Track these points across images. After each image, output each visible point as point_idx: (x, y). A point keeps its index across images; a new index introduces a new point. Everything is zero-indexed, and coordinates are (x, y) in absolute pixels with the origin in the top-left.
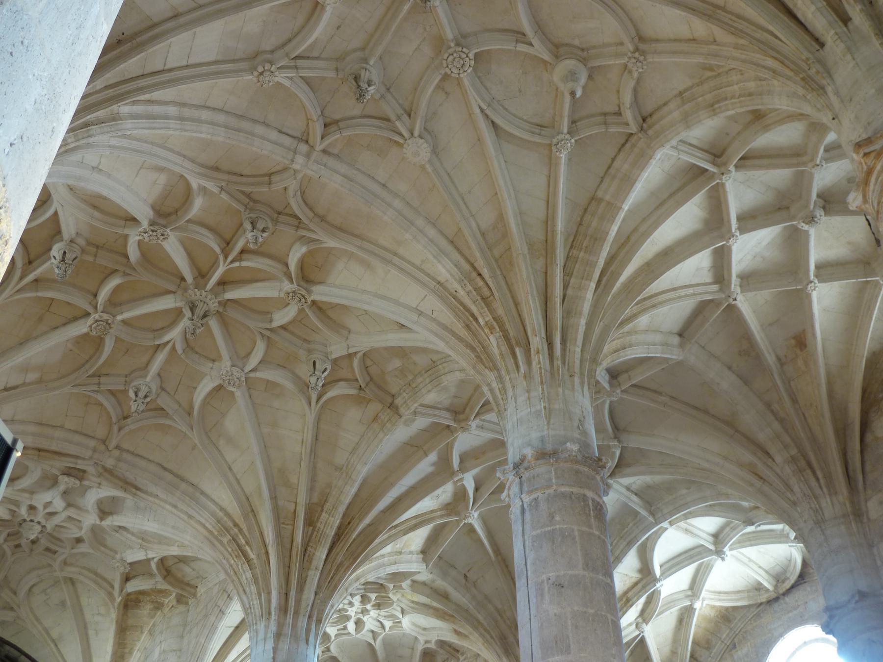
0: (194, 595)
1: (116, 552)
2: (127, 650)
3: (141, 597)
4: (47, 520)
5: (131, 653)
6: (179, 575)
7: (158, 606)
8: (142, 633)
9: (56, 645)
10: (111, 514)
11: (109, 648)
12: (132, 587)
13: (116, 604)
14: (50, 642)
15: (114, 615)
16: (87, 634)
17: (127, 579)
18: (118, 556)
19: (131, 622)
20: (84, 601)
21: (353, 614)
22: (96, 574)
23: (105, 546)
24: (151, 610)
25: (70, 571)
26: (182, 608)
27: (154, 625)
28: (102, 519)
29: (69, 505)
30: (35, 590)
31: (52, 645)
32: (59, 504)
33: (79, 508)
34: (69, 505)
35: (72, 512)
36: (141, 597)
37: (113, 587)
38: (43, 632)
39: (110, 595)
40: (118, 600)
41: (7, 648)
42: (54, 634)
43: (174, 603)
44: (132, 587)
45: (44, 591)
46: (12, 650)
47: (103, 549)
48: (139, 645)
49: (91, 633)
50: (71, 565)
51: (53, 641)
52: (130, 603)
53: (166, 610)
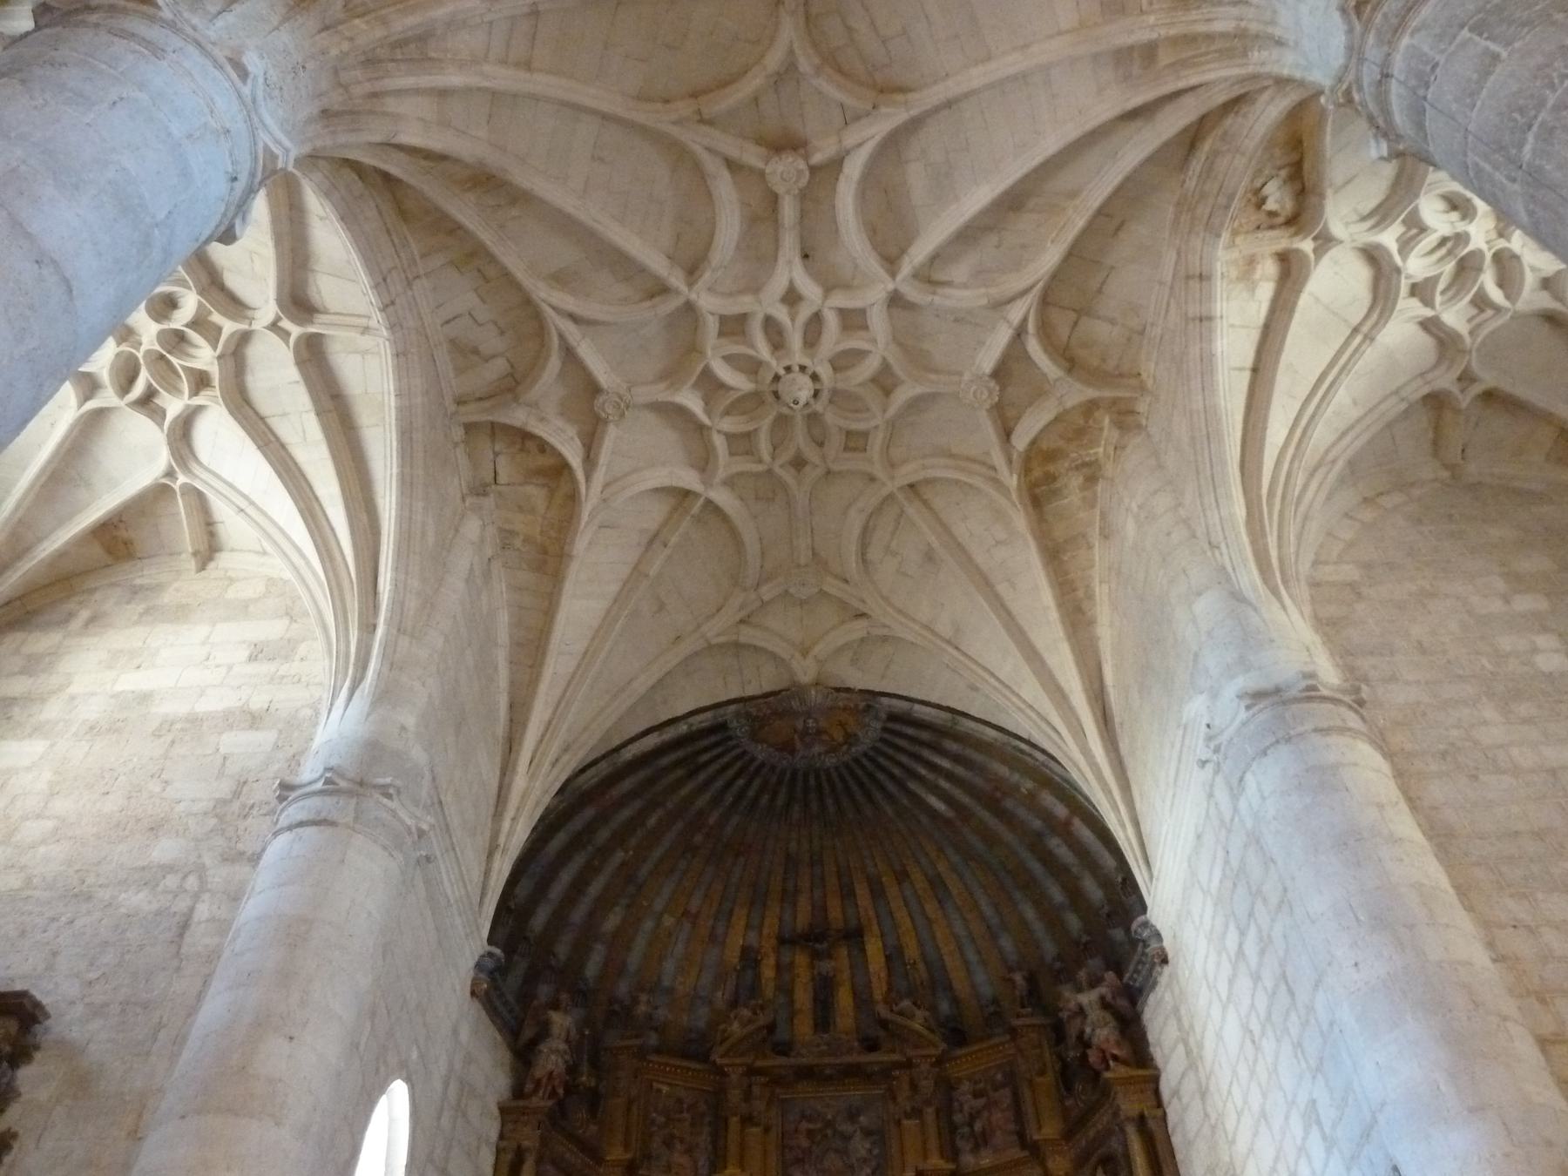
0: (1142, 388)
1: (960, 374)
2: (1080, 593)
3: (1051, 468)
4: (812, 357)
5: (1090, 596)
6: (1095, 362)
7: (1092, 474)
8: (1090, 547)
9: (957, 648)
10: (903, 251)
11: (1047, 597)
12: (1021, 441)
13: (1014, 496)
14: (944, 645)
15: (1020, 521)
16: (997, 597)
17: (1007, 434)
18: (967, 377)
19: (1060, 532)
20: (960, 531)
21: (1484, 247)
22: (952, 456)
23: (936, 371)
24: (1083, 488)
25: (909, 472)
26: (1135, 440)
27: (1103, 515)
28: (893, 275)
29: (828, 290)
30: (874, 553)
31: (950, 649)
32: (810, 290)
33: (847, 287)
34: (828, 290)
35: (840, 300)
36: (1051, 468)
37: (994, 468)
38: (925, 633)
39: (997, 483)
40: (1012, 481)
41: (885, 700)
42: (944, 628)
43: (1116, 434)
44: (1021, 441)
46: (895, 702)
47: (933, 377)
48: (1096, 573)
49: (1002, 588)
50: (904, 462)
51: (949, 642)
52: (1039, 495)
53: (1109, 469)
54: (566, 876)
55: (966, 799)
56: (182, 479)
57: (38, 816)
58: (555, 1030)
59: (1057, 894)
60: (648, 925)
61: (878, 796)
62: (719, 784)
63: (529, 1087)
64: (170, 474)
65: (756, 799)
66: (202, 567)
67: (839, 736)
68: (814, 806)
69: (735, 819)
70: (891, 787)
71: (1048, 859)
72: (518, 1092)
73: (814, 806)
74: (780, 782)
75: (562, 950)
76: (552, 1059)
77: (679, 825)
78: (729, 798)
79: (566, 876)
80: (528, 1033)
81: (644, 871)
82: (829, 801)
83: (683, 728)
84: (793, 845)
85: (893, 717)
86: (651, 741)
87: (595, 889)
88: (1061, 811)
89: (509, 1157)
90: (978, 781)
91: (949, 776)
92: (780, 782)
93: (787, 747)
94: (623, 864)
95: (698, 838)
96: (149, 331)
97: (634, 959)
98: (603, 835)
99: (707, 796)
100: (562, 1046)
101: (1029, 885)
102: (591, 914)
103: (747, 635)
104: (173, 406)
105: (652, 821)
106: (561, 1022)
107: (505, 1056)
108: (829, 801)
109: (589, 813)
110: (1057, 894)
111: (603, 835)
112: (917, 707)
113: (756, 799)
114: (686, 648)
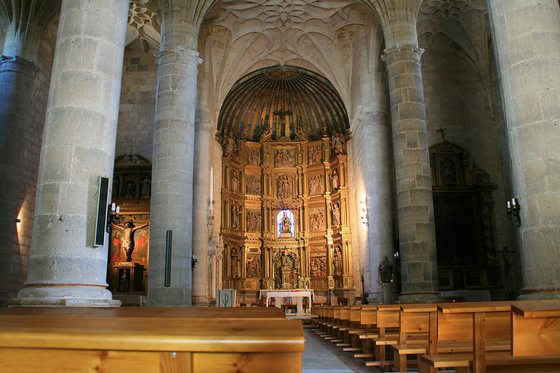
41: (300, 70)
45: (303, 42)
54: (228, 107)
55: (317, 90)
56: (142, 38)
57: (139, 124)
58: (230, 143)
59: (335, 113)
60: (245, 112)
61: (298, 86)
62: (261, 84)
63: (226, 154)
64: (139, 37)
65: (270, 85)
66: (146, 53)
67: (289, 75)
68: (283, 87)
69: (264, 90)
70: (301, 85)
71: (334, 106)
72: (224, 155)
73: (283, 87)
74: (275, 82)
75: (228, 122)
76: (230, 149)
77: (252, 92)
78: (263, 86)
79: (228, 107)
80: (225, 142)
81: (244, 102)
82: (286, 86)
83: (254, 75)
84: (277, 94)
85: (302, 73)
86: (247, 78)
87: (234, 108)
88: (337, 99)
89: (224, 168)
90: (321, 88)
91: (314, 85)
92: (275, 82)
93: (278, 76)
94: (240, 102)
95: (256, 94)
96: (135, 13)
97: (242, 120)
98: (236, 97)
99: (259, 86)
100: (232, 146)
101: (329, 109)
102: (233, 113)
103: (269, 57)
104: (139, 26)
105: (246, 92)
106: (231, 141)
107: (221, 147)
108: (286, 86)
109: (233, 94)
110: (335, 113)
111: (236, 97)
112: (308, 72)
113: (270, 85)
114: (255, 61)
